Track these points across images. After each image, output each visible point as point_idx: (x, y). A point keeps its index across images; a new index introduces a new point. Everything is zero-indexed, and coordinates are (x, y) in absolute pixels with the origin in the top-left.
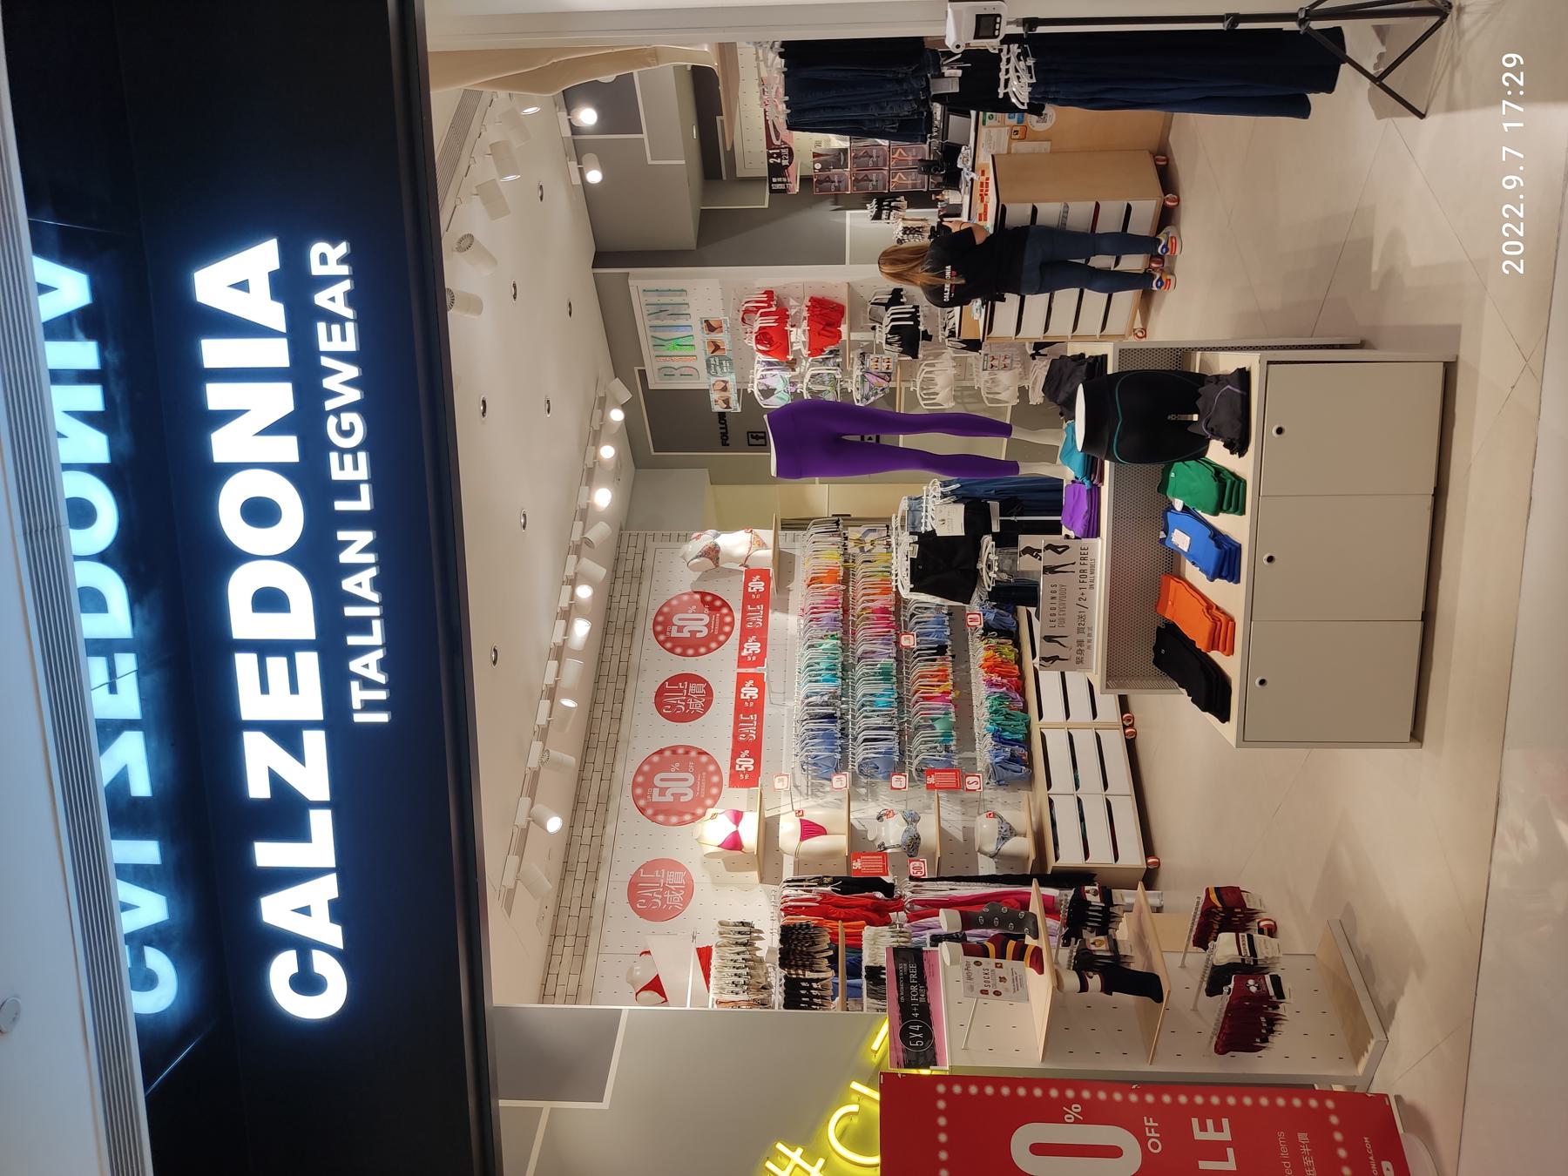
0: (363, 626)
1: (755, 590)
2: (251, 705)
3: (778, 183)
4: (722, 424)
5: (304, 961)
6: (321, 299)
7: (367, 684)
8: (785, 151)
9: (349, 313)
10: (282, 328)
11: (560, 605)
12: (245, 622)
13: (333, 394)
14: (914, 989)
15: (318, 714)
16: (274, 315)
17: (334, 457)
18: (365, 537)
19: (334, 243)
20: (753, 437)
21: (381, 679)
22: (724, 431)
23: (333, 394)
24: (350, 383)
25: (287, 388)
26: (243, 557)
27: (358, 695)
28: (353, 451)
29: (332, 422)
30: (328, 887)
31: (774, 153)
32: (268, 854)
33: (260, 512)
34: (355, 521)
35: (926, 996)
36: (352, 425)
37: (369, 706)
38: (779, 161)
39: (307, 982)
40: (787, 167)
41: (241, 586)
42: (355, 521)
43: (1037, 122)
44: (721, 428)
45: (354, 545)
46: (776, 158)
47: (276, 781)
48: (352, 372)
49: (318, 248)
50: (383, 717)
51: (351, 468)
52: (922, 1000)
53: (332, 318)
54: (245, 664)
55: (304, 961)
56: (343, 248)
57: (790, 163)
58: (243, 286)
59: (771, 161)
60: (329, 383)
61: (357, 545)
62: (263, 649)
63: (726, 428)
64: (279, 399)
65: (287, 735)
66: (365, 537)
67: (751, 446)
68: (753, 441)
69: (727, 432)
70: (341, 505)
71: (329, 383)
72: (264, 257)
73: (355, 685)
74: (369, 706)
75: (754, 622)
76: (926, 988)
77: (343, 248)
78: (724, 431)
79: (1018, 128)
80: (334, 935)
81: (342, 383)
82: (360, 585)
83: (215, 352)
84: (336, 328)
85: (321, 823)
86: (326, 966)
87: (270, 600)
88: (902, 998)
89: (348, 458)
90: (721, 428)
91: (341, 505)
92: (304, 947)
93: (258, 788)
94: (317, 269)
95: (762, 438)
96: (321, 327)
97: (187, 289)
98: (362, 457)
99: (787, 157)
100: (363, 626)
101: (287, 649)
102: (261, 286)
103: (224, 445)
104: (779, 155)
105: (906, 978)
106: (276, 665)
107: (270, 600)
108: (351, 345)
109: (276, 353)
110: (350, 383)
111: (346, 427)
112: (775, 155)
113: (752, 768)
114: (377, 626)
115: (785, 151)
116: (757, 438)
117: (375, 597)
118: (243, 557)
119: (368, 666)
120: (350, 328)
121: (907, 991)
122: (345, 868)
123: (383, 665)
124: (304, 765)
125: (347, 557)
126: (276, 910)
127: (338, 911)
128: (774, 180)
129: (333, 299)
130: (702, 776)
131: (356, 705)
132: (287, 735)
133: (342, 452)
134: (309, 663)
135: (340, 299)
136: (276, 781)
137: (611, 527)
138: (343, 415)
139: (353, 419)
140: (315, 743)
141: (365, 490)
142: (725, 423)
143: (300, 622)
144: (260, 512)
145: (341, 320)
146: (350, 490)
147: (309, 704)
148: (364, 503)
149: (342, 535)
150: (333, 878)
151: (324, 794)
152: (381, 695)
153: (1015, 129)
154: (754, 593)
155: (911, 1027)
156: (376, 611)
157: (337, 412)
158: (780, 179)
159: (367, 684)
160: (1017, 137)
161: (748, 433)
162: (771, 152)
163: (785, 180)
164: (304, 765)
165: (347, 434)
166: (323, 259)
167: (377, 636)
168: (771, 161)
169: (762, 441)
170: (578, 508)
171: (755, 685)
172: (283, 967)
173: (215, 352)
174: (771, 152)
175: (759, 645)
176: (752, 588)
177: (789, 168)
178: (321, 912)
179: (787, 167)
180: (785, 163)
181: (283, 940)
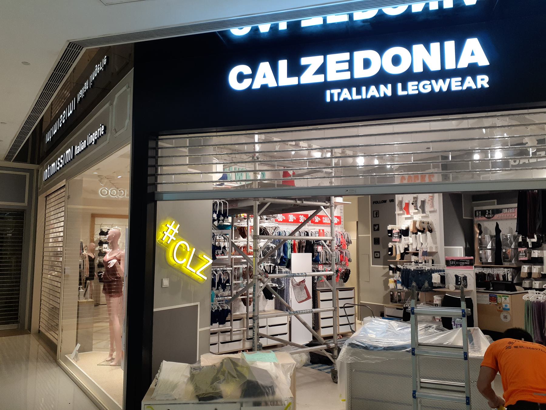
0: (359, 92)
1: (315, 219)
2: (332, 58)
3: (479, 213)
4: (382, 202)
5: (248, 76)
6: (469, 79)
7: (339, 94)
8: (491, 216)
9: (465, 88)
10: (460, 66)
11: (347, 150)
12: (359, 56)
13: (437, 82)
14: (463, 263)
15: (329, 79)
16: (463, 64)
17: (416, 83)
18: (389, 93)
19: (488, 83)
20: (377, 213)
21: (341, 99)
22: (379, 202)
23: (437, 82)
24: (441, 89)
25: (438, 68)
26: (381, 54)
27: (336, 92)
28: (418, 89)
29: (428, 82)
30: (272, 84)
31: (490, 212)
32: (283, 64)
33: (396, 60)
34: (394, 90)
35: (461, 266)
36: (426, 89)
37: (332, 95)
38: (487, 214)
39: (241, 77)
40: (485, 216)
41: (371, 54)
42: (394, 90)
43: (504, 315)
44: (380, 201)
45: (385, 91)
46: (488, 213)
47: (306, 67)
48: (445, 89)
49: (486, 78)
50: (328, 99)
51: (412, 88)
52: (461, 265)
53: (462, 82)
54: (346, 56)
55: (248, 76)
56: (487, 86)
57: (486, 218)
58: (473, 54)
59: (487, 211)
60: (441, 81)
61: (386, 90)
62: (351, 62)
63: (380, 203)
64: (435, 66)
65: (322, 70)
66: (389, 93)
67: (373, 212)
68: (375, 213)
69: (378, 203)
70: (400, 85)
71: (441, 81)
72: (483, 61)
73: (339, 90)
74: (332, 95)
75: (324, 220)
76: (463, 266)
77: (487, 86)
78: (379, 202)
79: (501, 308)
80: (257, 86)
81: (440, 86)
82: (373, 92)
83: (450, 45)
84: (460, 84)
85: (293, 81)
86: (246, 83)
87: (367, 64)
88: (460, 260)
89: (416, 88)
90: (380, 201)
91: (400, 85)
92: (252, 76)
93: (304, 61)
94: (479, 77)
95: (376, 216)
96: (460, 79)
97: (471, 36)
98: (417, 92)
99: (488, 217)
100: (359, 92)
101: (351, 69)
102: (473, 60)
103: (419, 48)
104: (489, 214)
105: (466, 262)
106: (346, 66)
107: (367, 64)
108: (454, 88)
109: (450, 65)
110: (441, 89)
111: (426, 87)
112: (489, 212)
113: (316, 221)
114: (359, 97)
115: (491, 216)
116: (376, 214)
117: (369, 96)
118: (381, 54)
119: (345, 94)
120: (460, 88)
121: (462, 261)
122: (278, 89)
123: (345, 100)
124: (313, 75)
125: (382, 87)
126: (264, 67)
127: (264, 87)
128: (480, 212)
129: (469, 82)
130: (479, 213)
131: (333, 91)
132: (322, 70)
133: (418, 85)
134: (347, 76)
135: (469, 85)
136: (306, 67)
137: (352, 163)
138: (430, 86)
139: (428, 89)
140: (320, 79)
141: (405, 93)
142: (382, 203)
143: (360, 73)
144: (396, 60)
145: (462, 85)
146: (404, 88)
147: (332, 76)
148: (400, 92)
149: (390, 86)
150: (276, 85)
151: (302, 82)
152: (336, 99)
153: (501, 307)
154: (315, 218)
155: (454, 262)
156: (364, 97)
157: (431, 84)
158: (480, 214)
159: (339, 94)
160: (498, 308)
161: (378, 211)
162: (491, 211)
163: (480, 216)
164: (313, 75)
165: (424, 87)
166: (482, 80)
167: (356, 97)
168: (487, 211)
169: (375, 216)
170: (345, 150)
171: (294, 220)
172: (246, 69)
173: (450, 45)
174: (491, 211)
175: (337, 222)
176: (316, 218)
177: (484, 217)
178: (264, 82)
179: (485, 216)
180: (486, 216)
181: (254, 69)
